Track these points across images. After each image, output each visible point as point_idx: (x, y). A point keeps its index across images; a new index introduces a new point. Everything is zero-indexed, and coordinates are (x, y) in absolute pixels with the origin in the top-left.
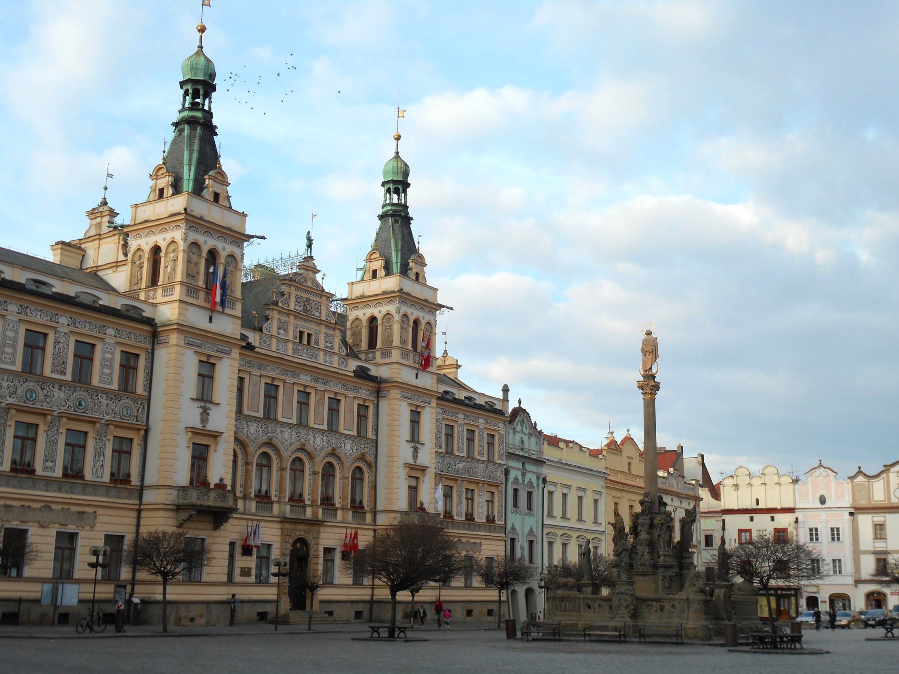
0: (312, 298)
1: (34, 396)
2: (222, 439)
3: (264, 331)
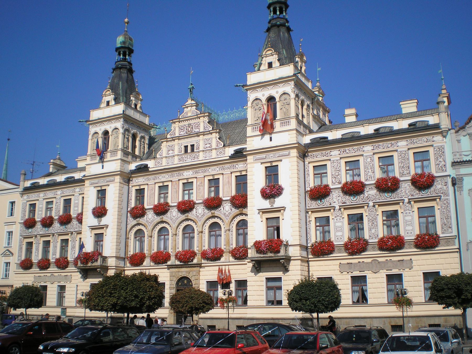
0: (191, 122)
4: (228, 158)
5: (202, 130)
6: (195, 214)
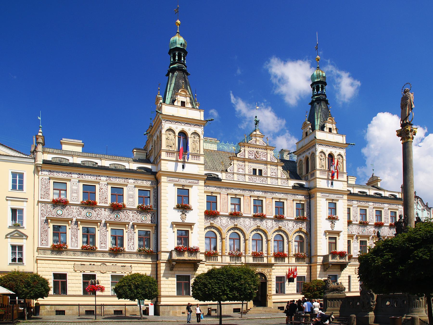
1: (91, 214)
2: (194, 227)
3: (229, 171)
4: (291, 188)
6: (265, 226)
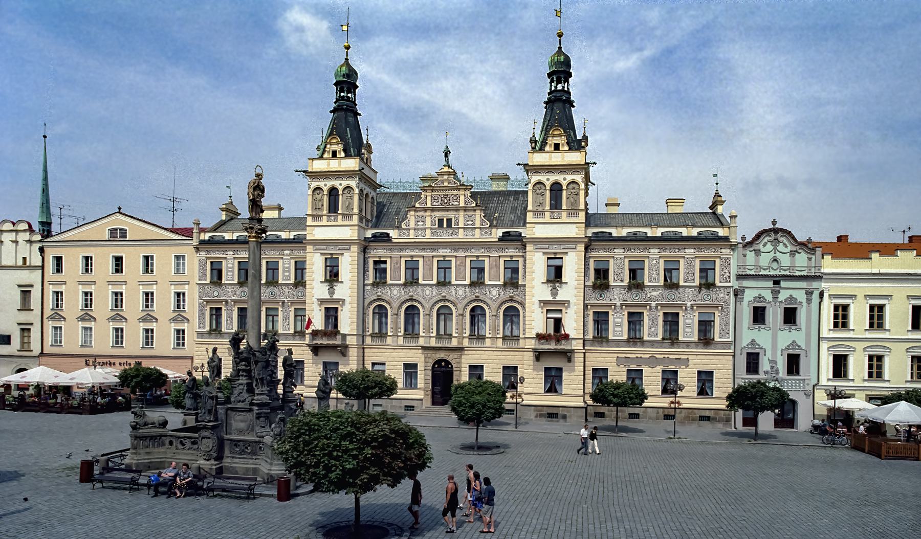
5: (462, 204)
